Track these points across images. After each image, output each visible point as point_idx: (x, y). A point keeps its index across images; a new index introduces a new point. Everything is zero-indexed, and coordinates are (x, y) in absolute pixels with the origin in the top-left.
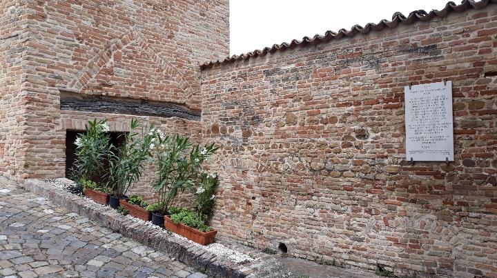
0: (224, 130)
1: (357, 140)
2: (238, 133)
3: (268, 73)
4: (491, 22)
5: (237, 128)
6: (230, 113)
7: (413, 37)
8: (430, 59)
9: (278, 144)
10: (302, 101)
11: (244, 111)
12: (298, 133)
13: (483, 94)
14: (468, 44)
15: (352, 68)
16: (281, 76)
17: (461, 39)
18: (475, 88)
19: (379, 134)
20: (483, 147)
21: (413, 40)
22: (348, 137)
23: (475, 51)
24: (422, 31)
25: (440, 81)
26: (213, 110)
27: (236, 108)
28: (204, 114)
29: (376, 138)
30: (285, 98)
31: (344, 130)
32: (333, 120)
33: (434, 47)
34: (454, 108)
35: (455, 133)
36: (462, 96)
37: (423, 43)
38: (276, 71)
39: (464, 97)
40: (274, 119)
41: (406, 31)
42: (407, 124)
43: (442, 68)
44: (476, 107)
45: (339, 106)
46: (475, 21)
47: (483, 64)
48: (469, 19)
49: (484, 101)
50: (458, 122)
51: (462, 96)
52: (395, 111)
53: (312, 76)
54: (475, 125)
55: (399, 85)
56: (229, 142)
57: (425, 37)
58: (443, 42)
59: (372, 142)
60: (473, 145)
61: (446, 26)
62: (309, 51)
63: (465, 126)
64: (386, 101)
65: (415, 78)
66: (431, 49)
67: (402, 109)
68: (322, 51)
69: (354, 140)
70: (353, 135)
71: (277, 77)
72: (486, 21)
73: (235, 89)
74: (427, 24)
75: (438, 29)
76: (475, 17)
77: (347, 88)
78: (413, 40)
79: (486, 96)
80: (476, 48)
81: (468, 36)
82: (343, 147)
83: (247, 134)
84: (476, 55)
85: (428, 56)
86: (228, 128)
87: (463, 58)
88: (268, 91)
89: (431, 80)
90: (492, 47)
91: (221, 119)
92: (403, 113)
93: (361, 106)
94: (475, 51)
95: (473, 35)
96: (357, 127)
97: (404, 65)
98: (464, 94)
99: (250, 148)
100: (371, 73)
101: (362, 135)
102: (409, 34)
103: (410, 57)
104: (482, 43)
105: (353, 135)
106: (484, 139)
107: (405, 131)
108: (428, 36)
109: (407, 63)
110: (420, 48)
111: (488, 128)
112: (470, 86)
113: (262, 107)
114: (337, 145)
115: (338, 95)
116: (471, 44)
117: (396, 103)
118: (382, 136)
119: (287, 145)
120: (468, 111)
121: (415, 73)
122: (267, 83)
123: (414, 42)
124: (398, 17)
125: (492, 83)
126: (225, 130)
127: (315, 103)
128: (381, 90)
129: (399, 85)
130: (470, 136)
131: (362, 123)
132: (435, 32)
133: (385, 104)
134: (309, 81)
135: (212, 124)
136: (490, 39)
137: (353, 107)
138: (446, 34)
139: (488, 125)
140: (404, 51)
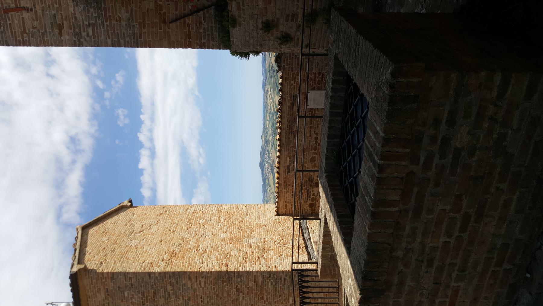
4: (289, 76)
6: (304, 196)
13: (315, 80)
17: (293, 86)
18: (312, 82)
33: (294, 96)
36: (314, 87)
37: (291, 100)
38: (288, 167)
46: (287, 82)
57: (289, 100)
68: (285, 144)
75: (287, 95)
81: (292, 84)
91: (307, 201)
98: (314, 86)
108: (289, 98)
110: (293, 101)
117: (313, 111)
120: (320, 85)
125: (312, 77)
132: (288, 96)
135: (308, 208)
137: (312, 130)
138: (289, 92)
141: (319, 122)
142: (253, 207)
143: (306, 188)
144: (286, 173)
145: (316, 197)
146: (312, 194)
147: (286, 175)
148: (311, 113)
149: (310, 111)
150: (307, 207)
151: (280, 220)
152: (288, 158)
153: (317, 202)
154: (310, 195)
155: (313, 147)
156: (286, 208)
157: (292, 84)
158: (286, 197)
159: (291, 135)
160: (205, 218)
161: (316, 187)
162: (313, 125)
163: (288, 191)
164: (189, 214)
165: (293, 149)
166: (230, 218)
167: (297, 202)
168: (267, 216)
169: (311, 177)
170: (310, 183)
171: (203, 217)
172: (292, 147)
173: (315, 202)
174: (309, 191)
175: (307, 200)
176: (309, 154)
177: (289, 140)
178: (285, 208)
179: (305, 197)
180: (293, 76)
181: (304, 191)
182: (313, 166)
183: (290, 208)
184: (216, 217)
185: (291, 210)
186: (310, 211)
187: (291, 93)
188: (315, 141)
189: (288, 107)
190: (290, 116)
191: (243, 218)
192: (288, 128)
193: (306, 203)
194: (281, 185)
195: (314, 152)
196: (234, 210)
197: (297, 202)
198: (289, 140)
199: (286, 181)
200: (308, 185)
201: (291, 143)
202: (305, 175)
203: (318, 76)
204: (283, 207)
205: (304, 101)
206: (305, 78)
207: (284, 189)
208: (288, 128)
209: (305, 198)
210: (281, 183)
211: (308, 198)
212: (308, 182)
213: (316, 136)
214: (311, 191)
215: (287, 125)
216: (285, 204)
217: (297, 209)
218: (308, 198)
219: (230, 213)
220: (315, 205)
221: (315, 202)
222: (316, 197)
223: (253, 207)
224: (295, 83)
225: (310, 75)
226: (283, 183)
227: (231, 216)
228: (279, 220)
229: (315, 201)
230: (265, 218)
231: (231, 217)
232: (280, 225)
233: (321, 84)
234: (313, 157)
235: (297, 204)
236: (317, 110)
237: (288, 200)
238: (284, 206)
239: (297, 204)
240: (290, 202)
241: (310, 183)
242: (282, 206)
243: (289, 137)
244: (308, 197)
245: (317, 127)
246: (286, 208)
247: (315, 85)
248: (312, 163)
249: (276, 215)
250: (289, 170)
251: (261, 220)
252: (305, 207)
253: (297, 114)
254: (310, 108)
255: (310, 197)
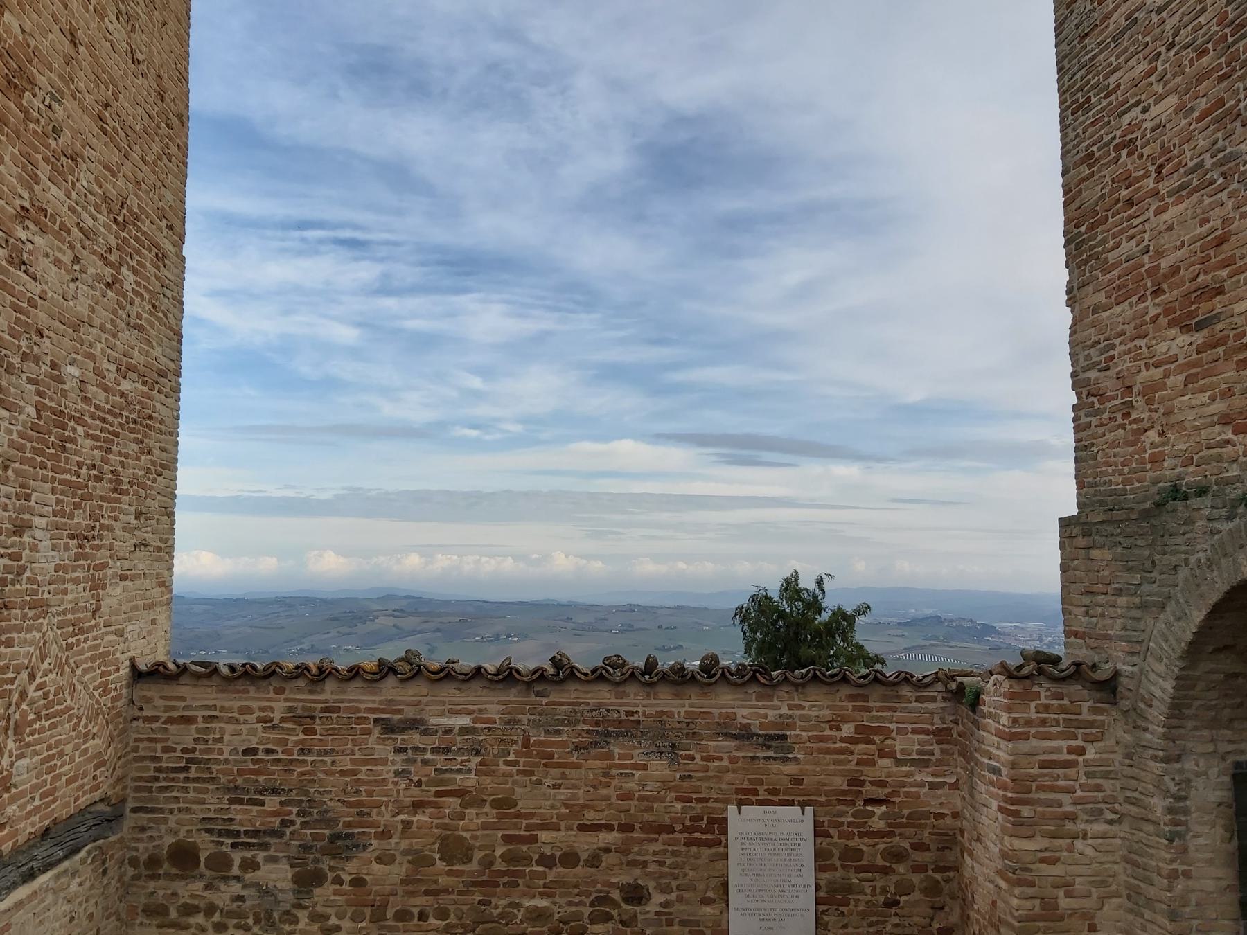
0: (220, 863)
1: (625, 906)
2: (278, 875)
3: (389, 728)
4: (874, 713)
5: (273, 860)
6: (244, 816)
7: (745, 712)
8: (775, 759)
9: (415, 911)
10: (487, 808)
11: (301, 814)
12: (474, 884)
13: (861, 835)
14: (839, 745)
15: (617, 751)
16: (429, 739)
17: (828, 732)
18: (850, 824)
19: (673, 896)
20: (860, 930)
21: (744, 717)
22: (603, 899)
23: (851, 758)
24: (760, 704)
25: (791, 803)
26: (168, 800)
27: (272, 803)
28: (134, 810)
29: (666, 904)
30: (439, 794)
31: (594, 882)
32: (570, 859)
34: (818, 855)
35: (818, 902)
36: (828, 835)
37: (762, 725)
38: (415, 724)
39: (832, 838)
40: (404, 844)
41: (730, 697)
42: (733, 880)
43: (796, 781)
44: (851, 856)
45: (582, 828)
47: (862, 784)
48: (841, 700)
49: (864, 848)
50: (822, 883)
51: (828, 835)
52: (707, 852)
53: (516, 753)
54: (849, 889)
55: (716, 800)
56: (240, 898)
57: (766, 716)
58: (797, 732)
59: (657, 913)
60: (845, 926)
61: (803, 703)
62: (512, 695)
63: (833, 888)
64: (687, 829)
65: (746, 792)
66: (776, 740)
67: (721, 849)
68: (545, 700)
69: (615, 904)
70: (616, 895)
71: (415, 738)
72: (868, 709)
73: (268, 751)
74: (769, 691)
75: (790, 707)
76: (852, 698)
77: (603, 792)
78: (744, 717)
79: (866, 840)
80: (852, 753)
81: (839, 729)
82: (592, 922)
83: (307, 880)
84: (852, 766)
85: (771, 754)
86: (237, 857)
87: (833, 767)
88: (388, 772)
89: (776, 799)
90: (876, 757)
91: (208, 831)
92: (725, 856)
93: (635, 835)
94: (851, 758)
95: (848, 730)
96: (625, 878)
97: (725, 763)
98: (832, 831)
99: (315, 917)
100: (659, 768)
101: (635, 895)
102: (736, 703)
103: (738, 748)
104: (861, 746)
105: (616, 895)
106: (863, 915)
107: (726, 893)
108: (772, 714)
109: (733, 760)
111: (869, 898)
112: (841, 820)
113: (363, 810)
114: (577, 916)
115: (584, 807)
116: (844, 745)
117: (710, 836)
118: (680, 900)
119: (442, 914)
120: (838, 863)
121: (746, 783)
122: (384, 751)
123: (745, 721)
124: (723, 672)
125: (875, 819)
126: (228, 864)
127: (519, 816)
128: (679, 806)
129: (716, 800)
130: (841, 908)
131: (637, 871)
132: (785, 710)
133: (687, 835)
134: (507, 763)
135: (169, 840)
136: (872, 742)
137: (615, 834)
138: (803, 718)
139: (868, 891)
140: (726, 735)
141: (652, 868)
142: (163, 546)
143: (292, 823)
144: (382, 711)
145: (237, 878)
146: (254, 857)
147: (372, 716)
148: (704, 824)
149: (712, 821)
150: (176, 833)
151: (112, 694)
152: (464, 721)
153: (206, 887)
154: (247, 846)
155: (525, 848)
156: (170, 721)
157: (839, 729)
158: (242, 718)
159: (588, 732)
160: (137, 300)
161: (293, 876)
162: (640, 842)
163: (274, 727)
164: (154, 227)
165: (516, 742)
166: (131, 425)
167: (205, 780)
168: (130, 620)
169: (357, 846)
170: (319, 845)
171: (142, 291)
172: (526, 744)
173: (202, 876)
174: (273, 841)
175: (220, 833)
176: (484, 827)
177: (561, 722)
178: (176, 714)
179: (238, 817)
180: (877, 731)
181: (275, 814)
182: (418, 852)
183: (169, 744)
184: (138, 358)
185: (159, 746)
186: (147, 849)
187: (798, 723)
188: (558, 854)
189: (730, 710)
190: (688, 724)
191: (126, 493)
192: (628, 713)
193: (200, 826)
194: (311, 692)
195: (498, 852)
196: (157, 452)
197: (205, 780)
198: (561, 722)
199: (335, 716)
200: (308, 832)
201: (547, 732)
202: (369, 814)
203: (882, 847)
204: (183, 704)
205: (761, 789)
206: (868, 787)
207: (290, 709)
208: (623, 717)
209: (232, 820)
210: (322, 691)
211: (229, 834)
212: (327, 832)
213: (584, 856)
214: (272, 852)
215: (640, 709)
216: (200, 714)
217: (164, 779)
218: (229, 834)
219: (148, 426)
220: (182, 878)
221: (202, 876)
222: (237, 878)
223: (163, 546)
224: (842, 740)
225: (884, 808)
226: (326, 701)
227: (139, 432)
228: (113, 686)
229: (208, 873)
230: (123, 608)
231: (132, 431)
232: (96, 693)
233: (843, 867)
234: (470, 848)
235: (196, 780)
236: (716, 854)
237: (222, 730)
238: (186, 708)
239: (196, 780)
240: (206, 741)
241: (319, 845)
242: (183, 699)
243: (577, 722)
244: (237, 834)
245: (631, 857)
246: (170, 721)
247: (836, 837)
248: (437, 846)
249: (133, 666)
250: (402, 730)
251: (118, 590)
252: (172, 824)
253: (698, 757)
254: (726, 819)
255: (234, 845)
